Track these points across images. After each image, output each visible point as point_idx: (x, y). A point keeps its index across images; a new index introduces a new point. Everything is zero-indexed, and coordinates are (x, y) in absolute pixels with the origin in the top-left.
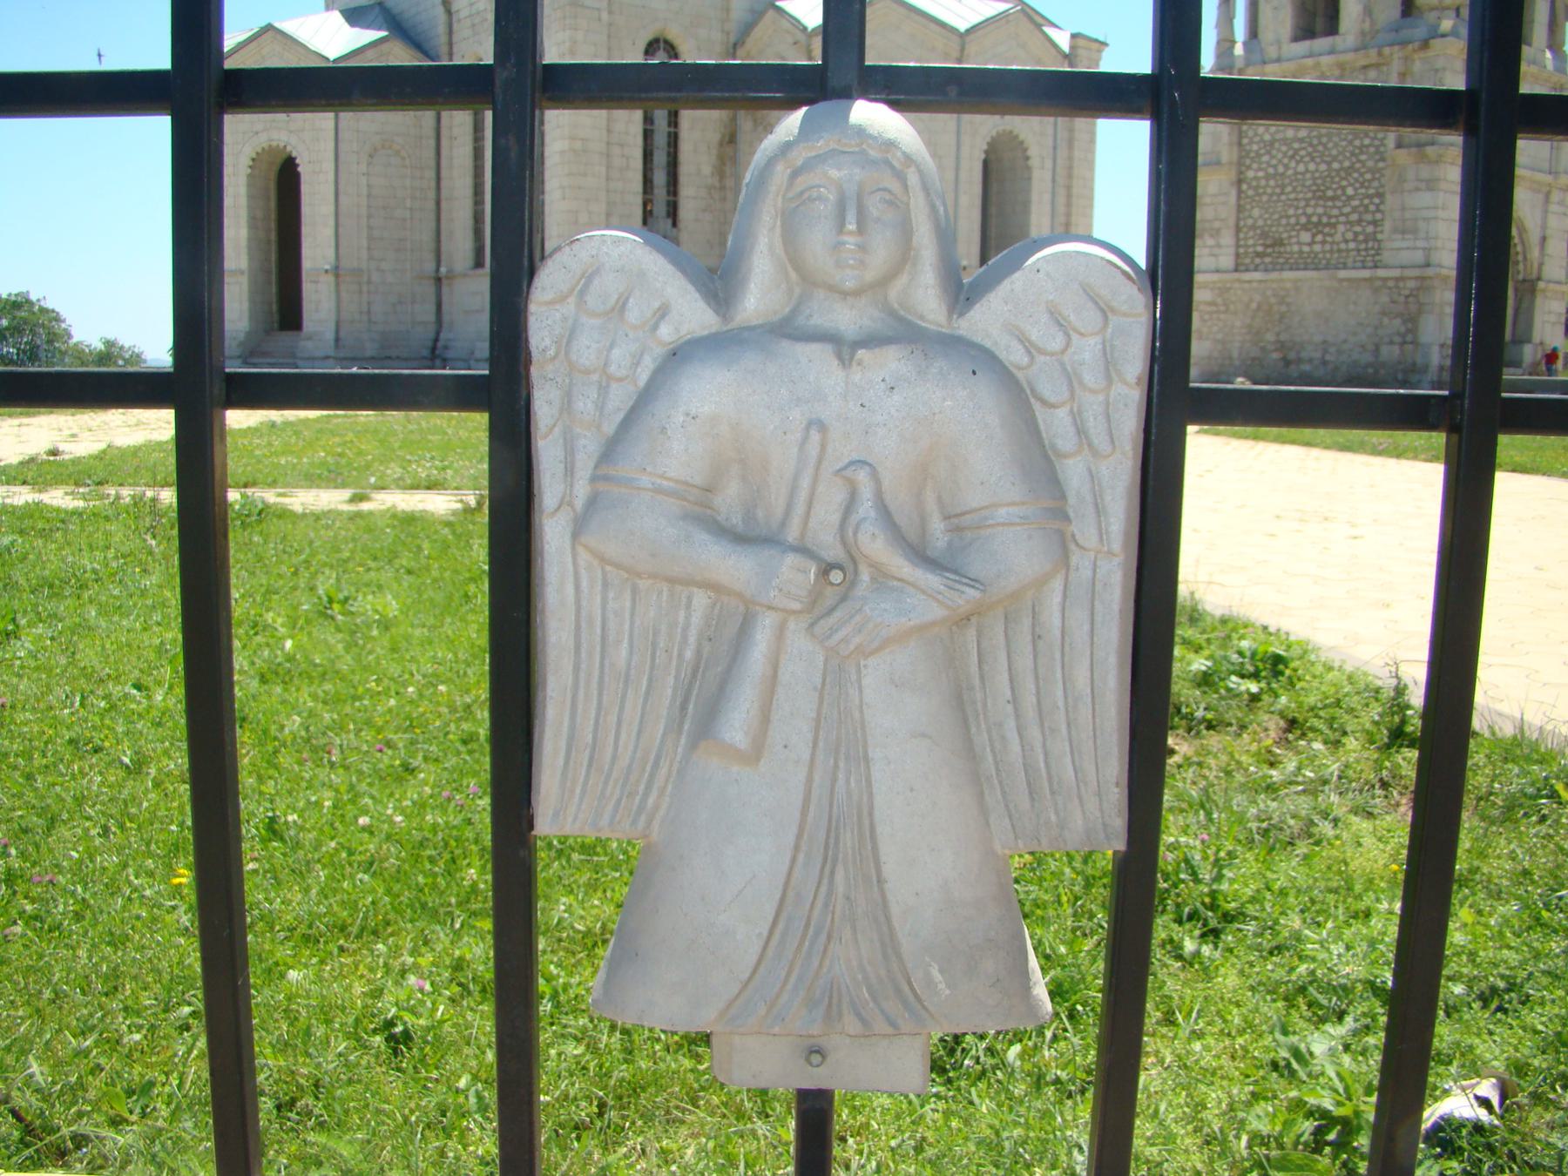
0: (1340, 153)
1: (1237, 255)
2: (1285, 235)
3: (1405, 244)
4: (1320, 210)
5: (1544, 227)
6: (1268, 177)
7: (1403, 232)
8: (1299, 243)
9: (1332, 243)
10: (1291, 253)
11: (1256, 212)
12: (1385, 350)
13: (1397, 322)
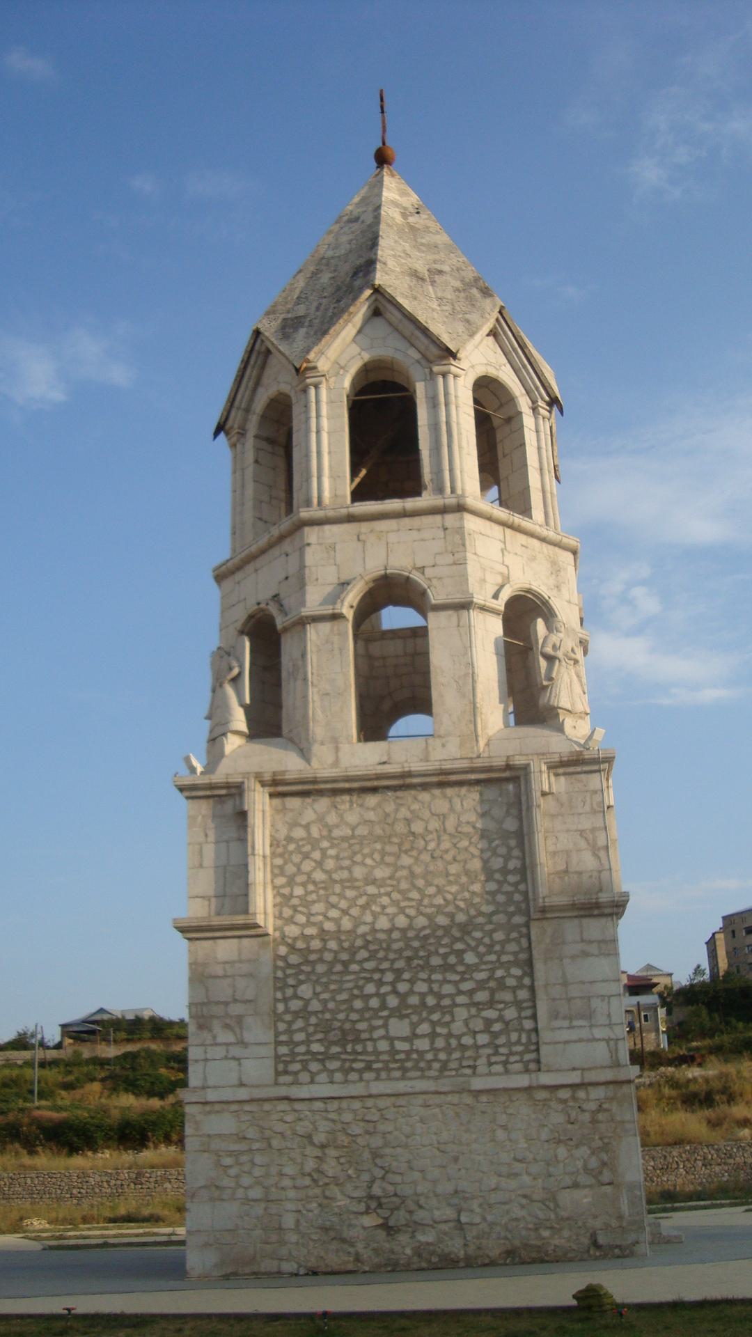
1: (277, 1057)
2: (362, 1026)
3: (574, 1035)
4: (421, 987)
8: (391, 1040)
10: (377, 1053)
12: (566, 1198)
13: (584, 1151)
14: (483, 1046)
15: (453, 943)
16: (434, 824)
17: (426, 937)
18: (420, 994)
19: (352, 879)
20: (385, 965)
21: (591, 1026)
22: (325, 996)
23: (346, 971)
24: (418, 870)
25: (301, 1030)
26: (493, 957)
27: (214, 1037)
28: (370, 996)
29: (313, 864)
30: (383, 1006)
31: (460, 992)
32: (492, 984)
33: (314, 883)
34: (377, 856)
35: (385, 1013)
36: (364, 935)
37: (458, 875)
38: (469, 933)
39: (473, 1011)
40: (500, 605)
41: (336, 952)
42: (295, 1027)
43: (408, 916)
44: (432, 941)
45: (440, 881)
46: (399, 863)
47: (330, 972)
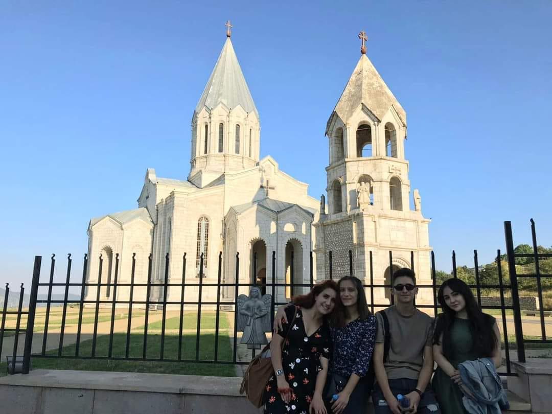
1: (326, 274)
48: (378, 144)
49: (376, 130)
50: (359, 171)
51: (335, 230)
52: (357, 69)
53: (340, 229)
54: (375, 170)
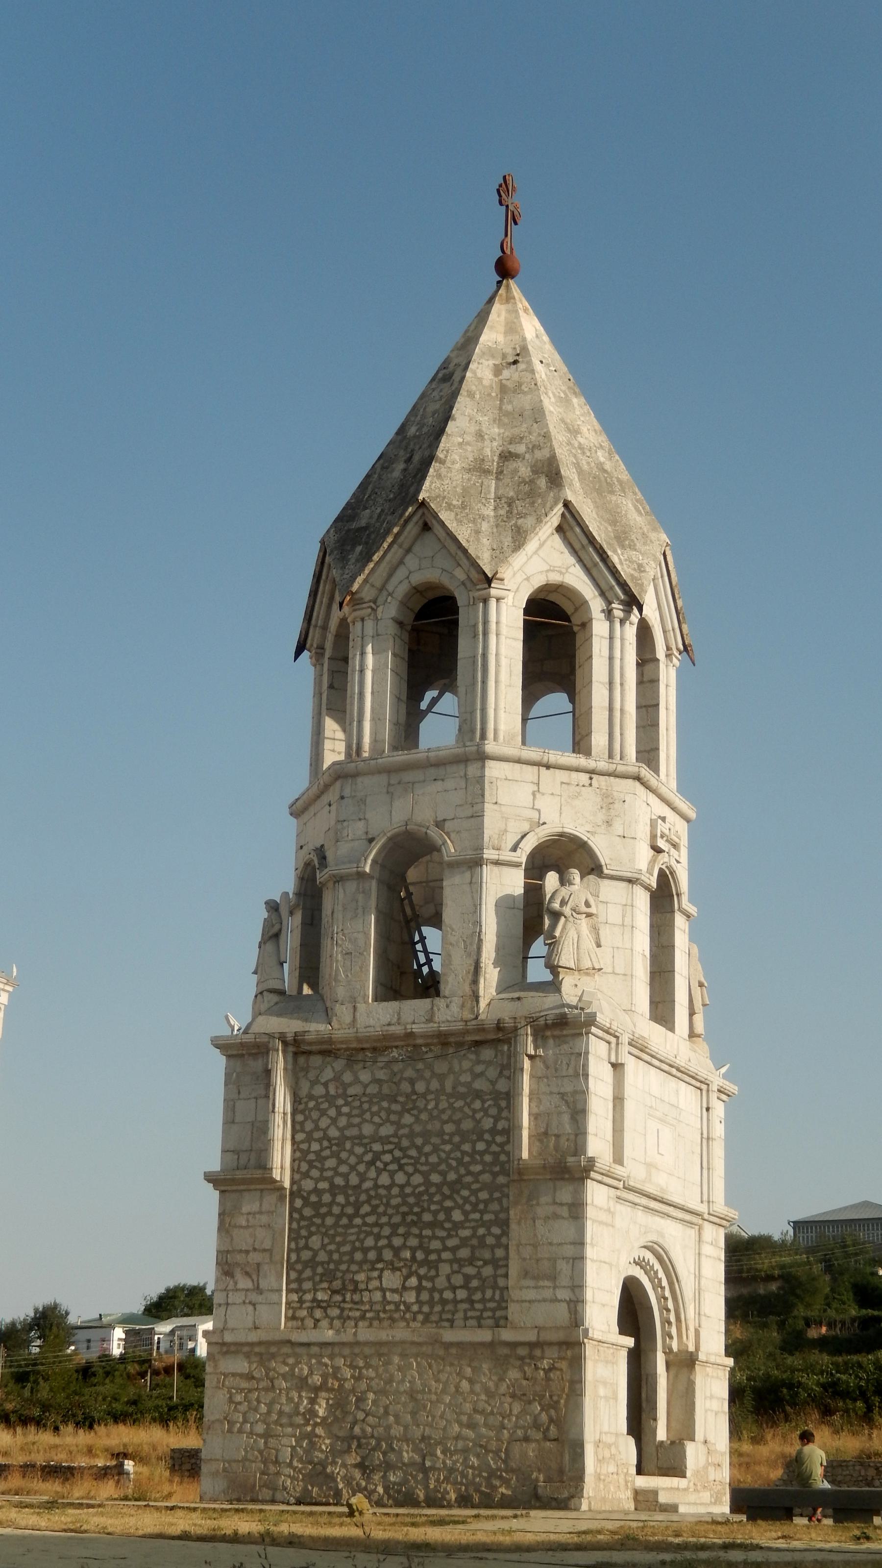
0: (441, 1161)
4: (413, 1242)
5: (699, 1276)
6: (334, 1190)
7: (536, 1278)
8: (383, 1290)
9: (433, 1290)
10: (371, 1303)
11: (315, 1242)
12: (516, 1448)
14: (462, 1301)
15: (443, 1200)
16: (435, 1085)
17: (421, 1194)
18: (411, 1248)
19: (361, 1137)
20: (384, 1220)
21: (555, 1288)
22: (332, 1247)
23: (350, 1225)
24: (418, 1128)
25: (309, 1279)
26: (476, 1216)
27: (236, 1283)
28: (369, 1249)
29: (329, 1121)
30: (380, 1259)
31: (445, 1248)
32: (474, 1242)
33: (329, 1140)
34: (383, 1114)
35: (380, 1266)
36: (367, 1191)
37: (452, 1135)
38: (458, 1192)
39: (456, 1267)
40: (522, 856)
41: (343, 1206)
42: (304, 1275)
43: (406, 1173)
44: (426, 1197)
45: (435, 1140)
46: (403, 1121)
47: (336, 1225)
48: (617, 705)
49: (611, 638)
50: (539, 811)
51: (379, 1082)
52: (492, 336)
53: (412, 1082)
54: (608, 823)
